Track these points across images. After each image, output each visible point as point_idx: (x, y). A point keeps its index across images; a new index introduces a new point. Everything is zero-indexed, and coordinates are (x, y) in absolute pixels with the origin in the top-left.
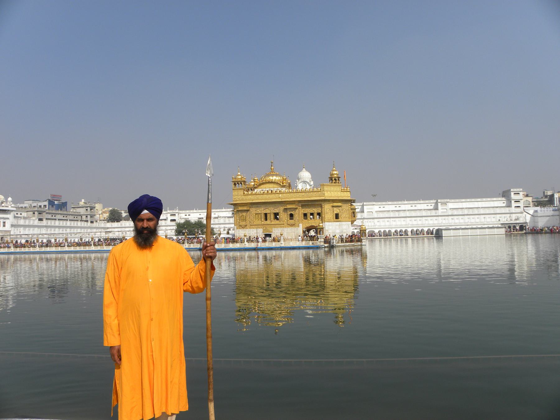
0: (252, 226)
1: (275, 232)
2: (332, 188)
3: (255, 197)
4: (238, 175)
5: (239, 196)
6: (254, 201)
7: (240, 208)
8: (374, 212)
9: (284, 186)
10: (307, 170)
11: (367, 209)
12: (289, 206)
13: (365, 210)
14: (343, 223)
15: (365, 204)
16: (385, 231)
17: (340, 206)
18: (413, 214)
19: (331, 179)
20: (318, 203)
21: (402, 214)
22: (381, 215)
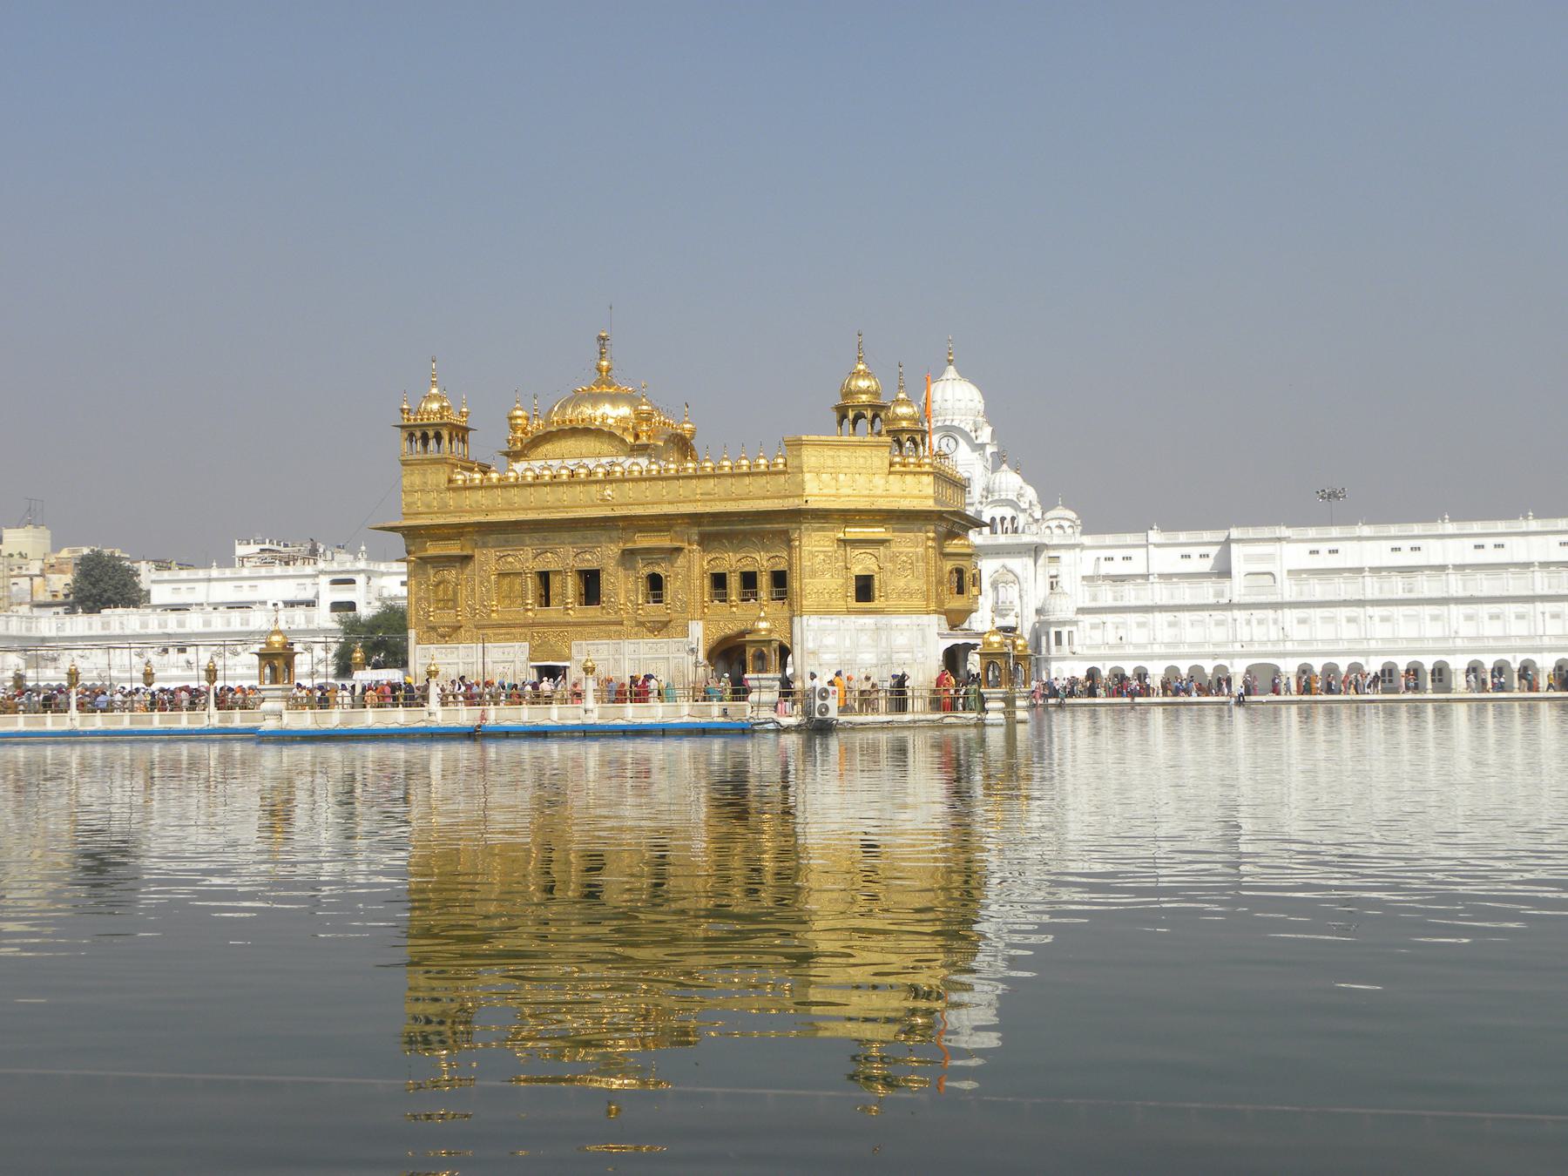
0: (486, 630)
2: (844, 456)
3: (499, 497)
4: (431, 398)
5: (431, 495)
6: (492, 518)
7: (433, 550)
8: (1282, 576)
9: (639, 450)
10: (964, 374)
11: (1248, 558)
12: (643, 541)
13: (1239, 566)
14: (897, 620)
15: (1235, 533)
16: (1330, 670)
17: (882, 542)
18: (1485, 585)
19: (842, 412)
20: (779, 525)
21: (1426, 586)
22: (1318, 590)
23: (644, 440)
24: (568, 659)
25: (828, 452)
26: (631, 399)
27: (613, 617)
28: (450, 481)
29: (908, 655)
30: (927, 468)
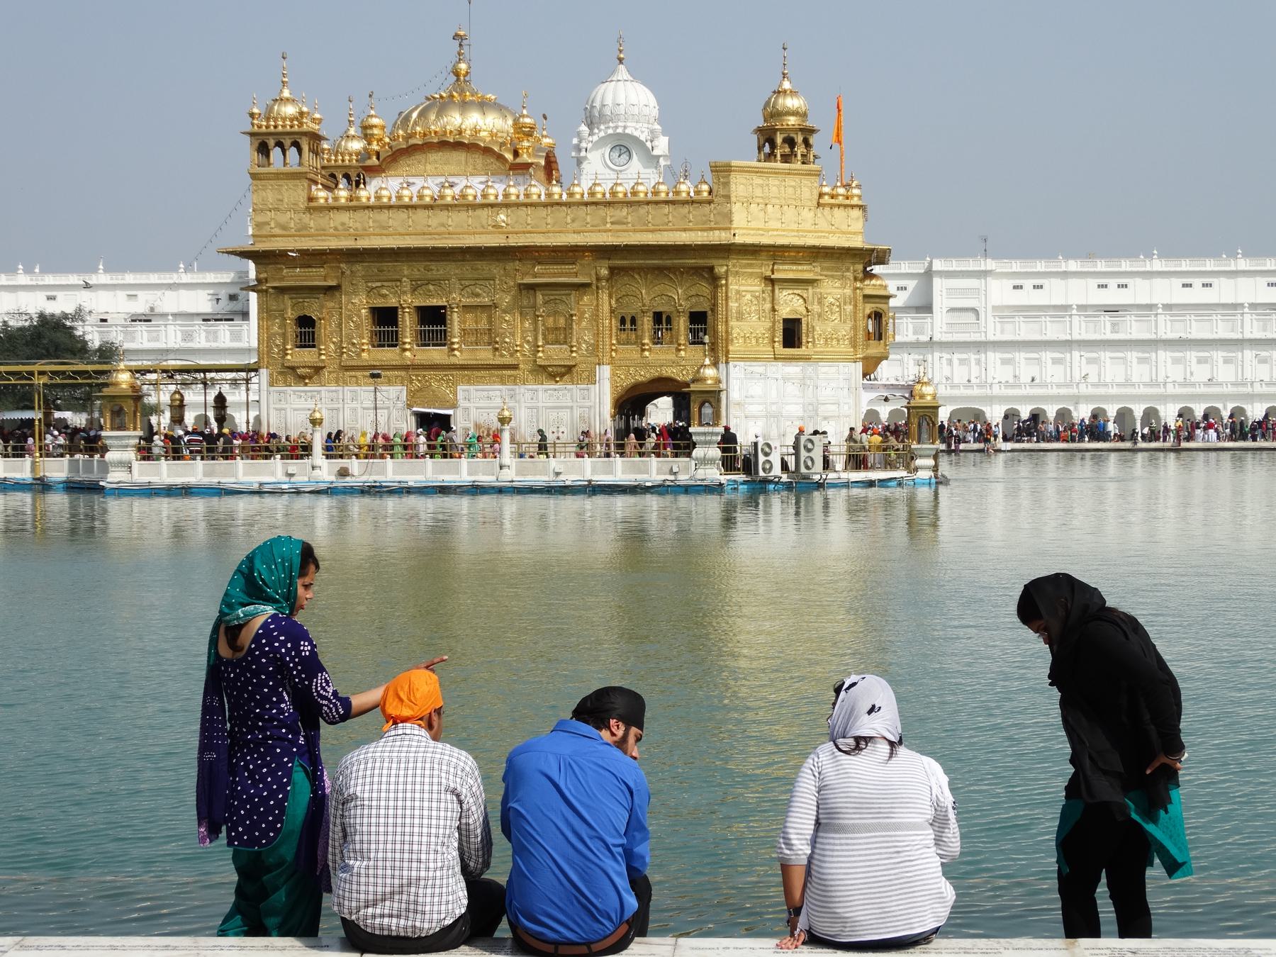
1: (473, 406)
3: (370, 219)
6: (363, 244)
10: (636, 76)
14: (825, 369)
15: (938, 265)
18: (1197, 329)
20: (702, 264)
21: (1134, 329)
22: (1026, 331)
23: (525, 158)
24: (454, 406)
25: (758, 180)
26: (498, 107)
27: (508, 360)
28: (311, 199)
29: (834, 407)
30: (855, 201)
